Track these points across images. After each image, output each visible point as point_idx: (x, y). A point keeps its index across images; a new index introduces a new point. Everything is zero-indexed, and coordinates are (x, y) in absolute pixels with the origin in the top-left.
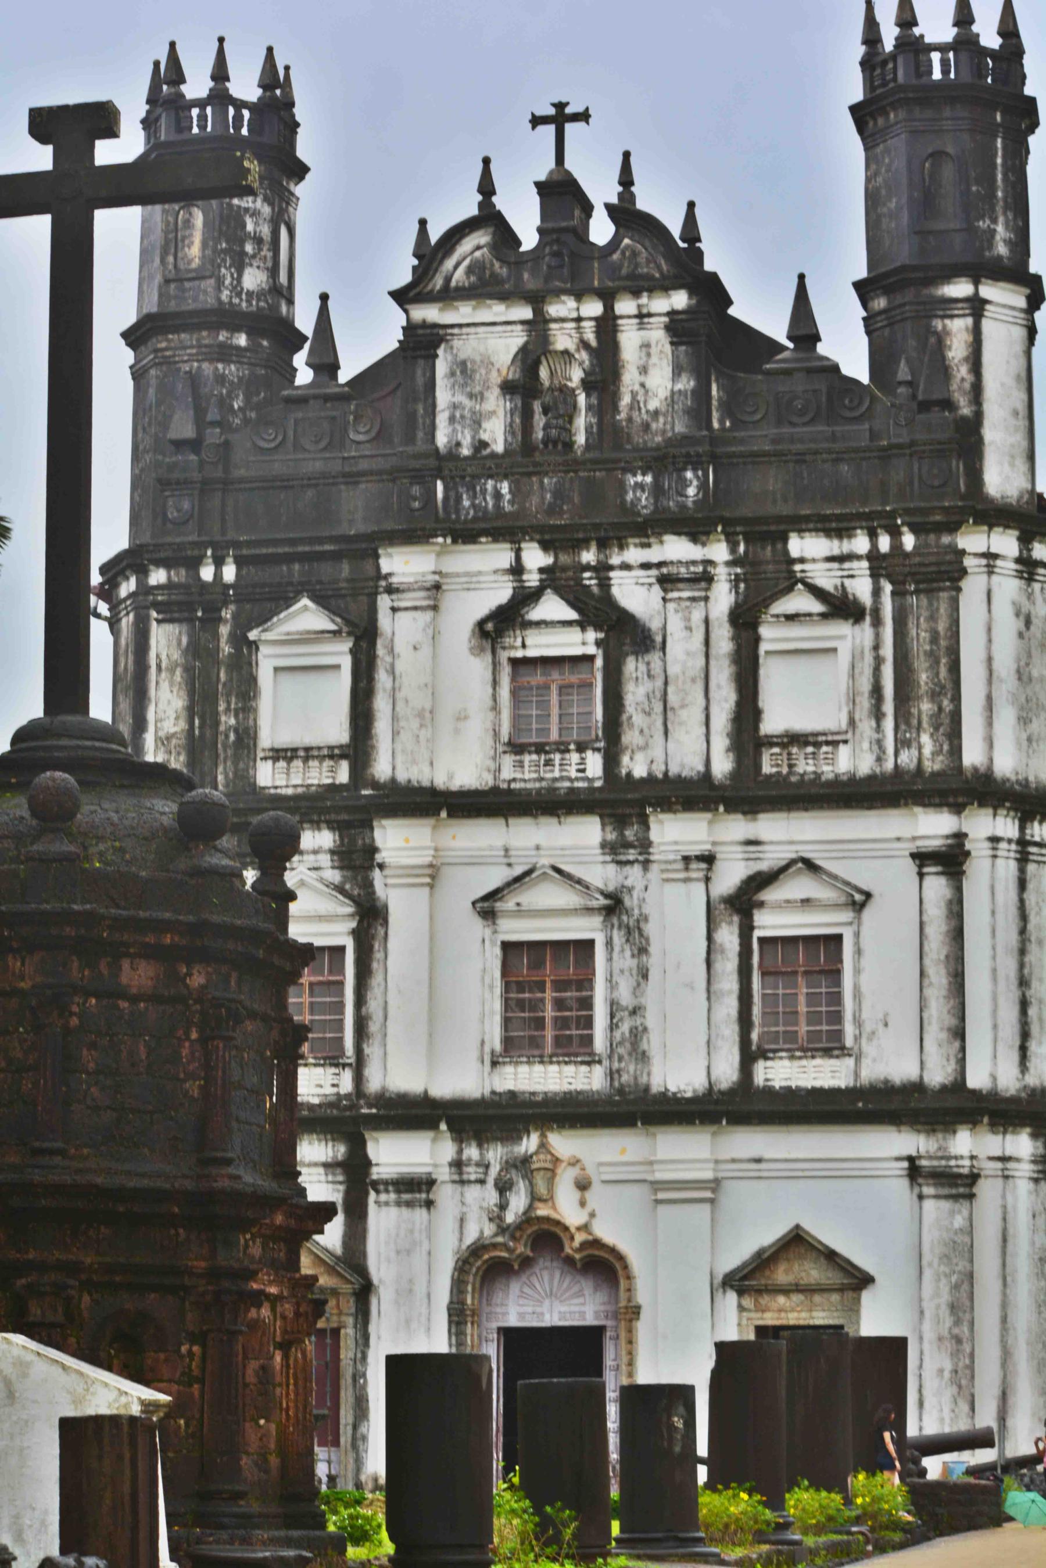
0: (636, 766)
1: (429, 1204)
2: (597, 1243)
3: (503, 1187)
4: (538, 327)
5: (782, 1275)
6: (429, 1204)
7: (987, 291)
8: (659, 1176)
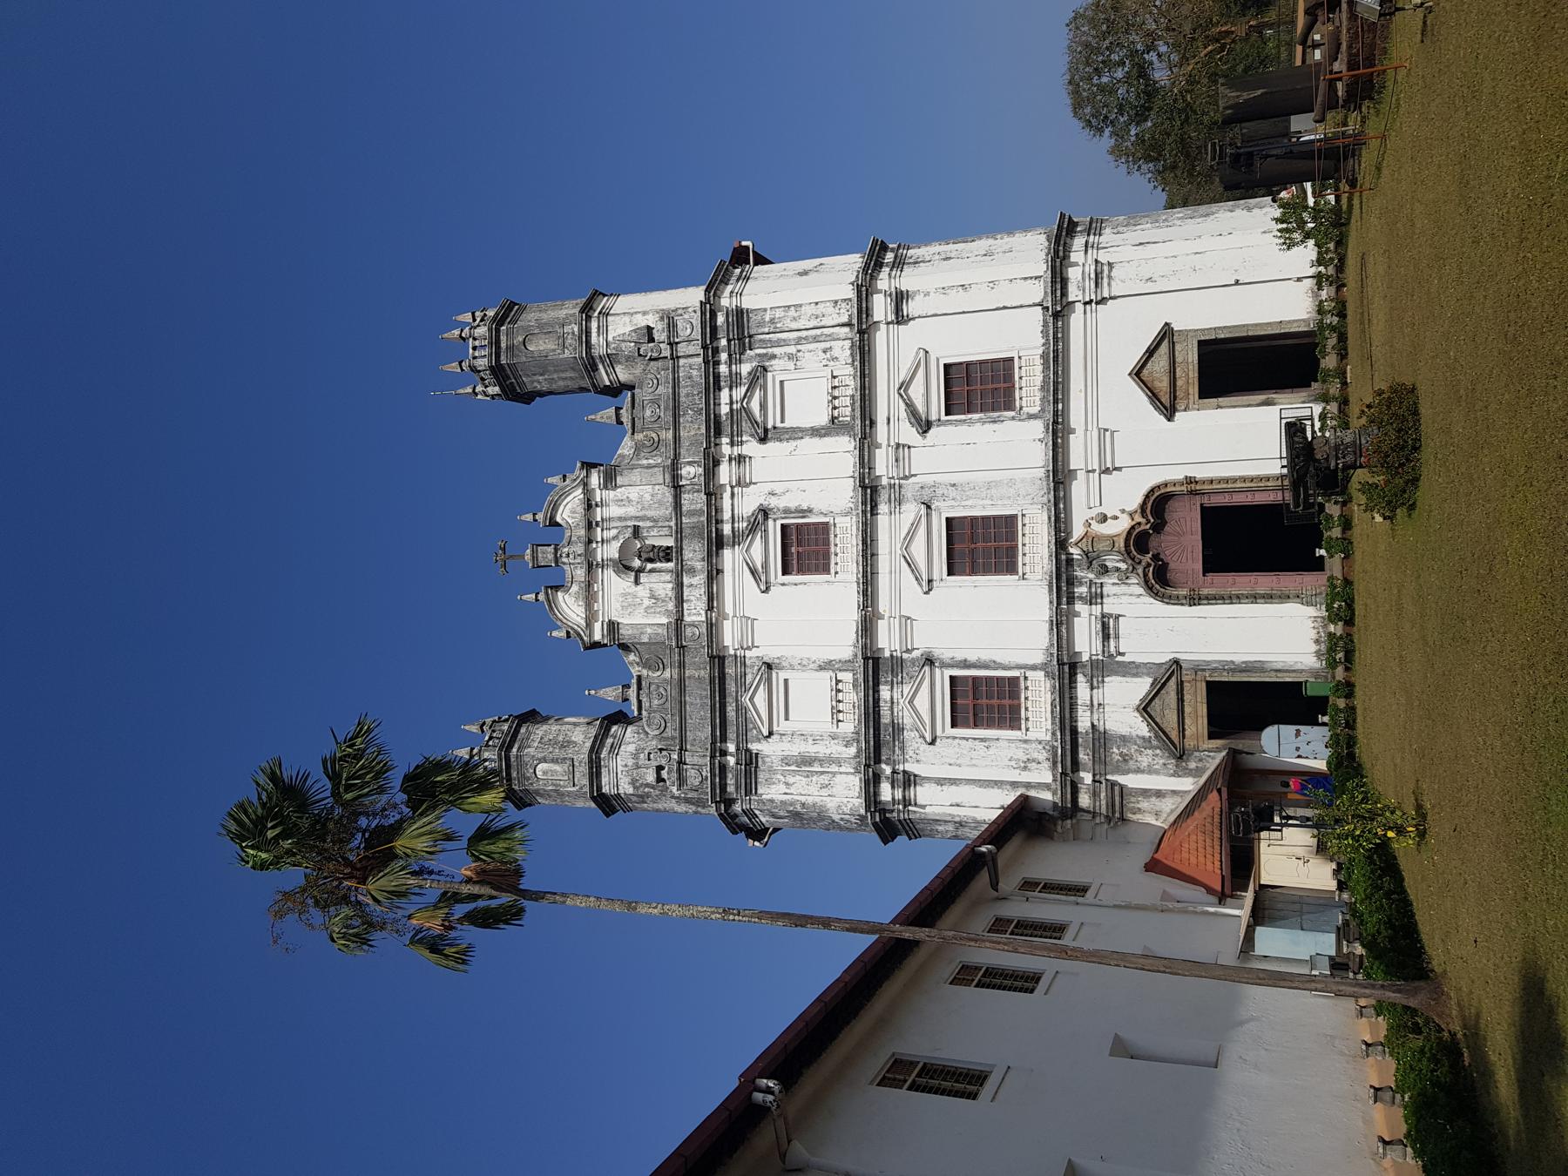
1: (1117, 617)
3: (1105, 570)
6: (1117, 617)
8: (1096, 467)
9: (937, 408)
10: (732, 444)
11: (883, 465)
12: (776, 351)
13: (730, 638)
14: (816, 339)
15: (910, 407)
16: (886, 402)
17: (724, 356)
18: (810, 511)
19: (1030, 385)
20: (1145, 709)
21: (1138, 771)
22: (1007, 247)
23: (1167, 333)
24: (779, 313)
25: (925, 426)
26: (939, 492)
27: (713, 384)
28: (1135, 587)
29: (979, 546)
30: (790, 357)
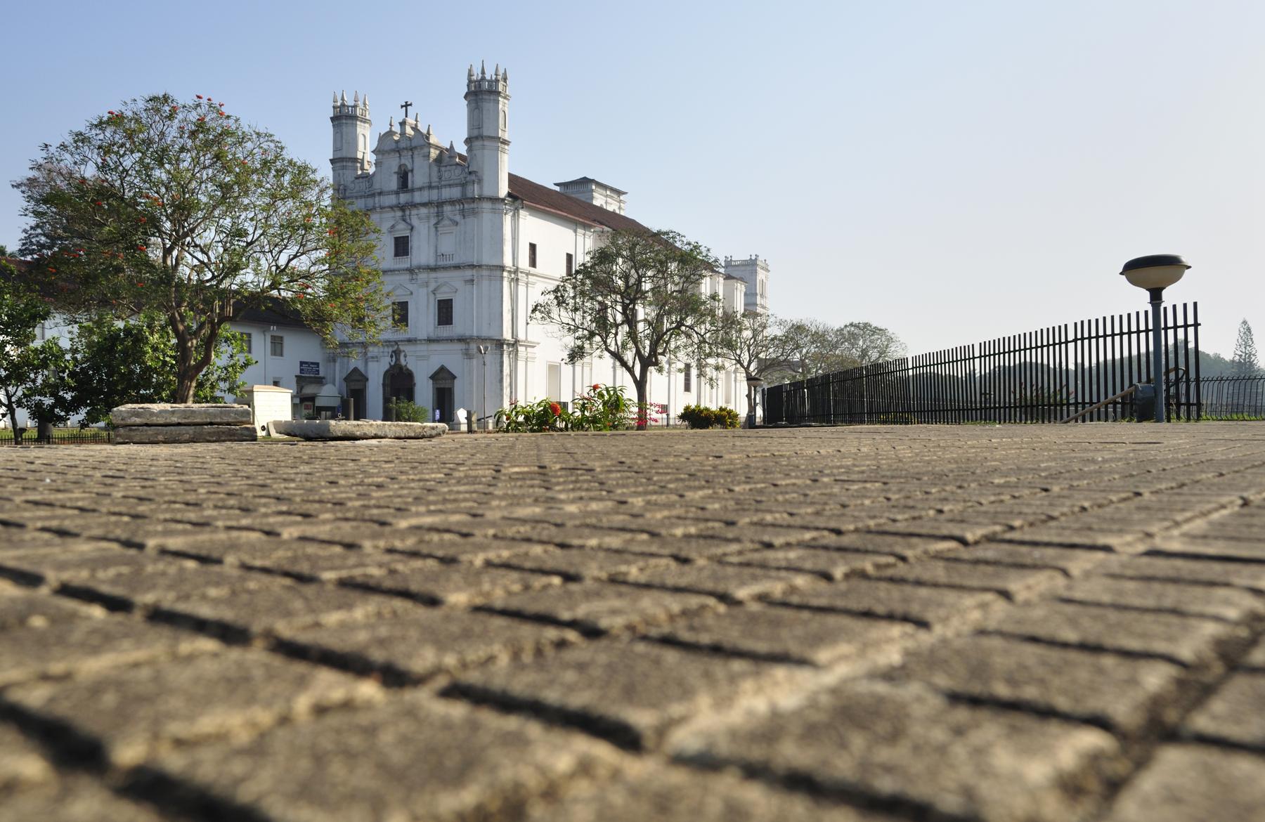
0: (415, 263)
7: (486, 143)
11: (423, 276)
19: (445, 331)
20: (356, 370)
27: (452, 202)
28: (387, 367)
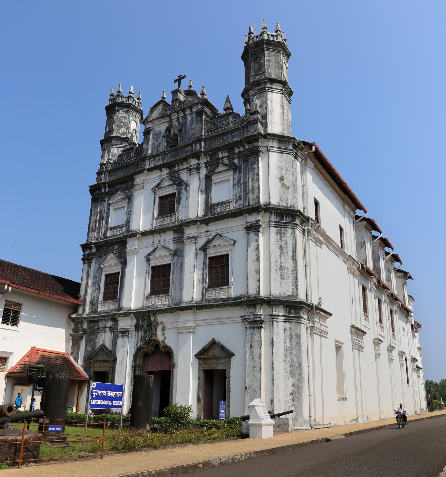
2: (166, 346)
3: (146, 331)
4: (171, 121)
5: (210, 354)
8: (179, 326)
9: (212, 253)
10: (205, 163)
12: (242, 175)
13: (139, 179)
14: (245, 191)
15: (212, 239)
16: (214, 228)
17: (241, 149)
18: (179, 203)
21: (86, 346)
22: (285, 277)
23: (229, 355)
24: (256, 171)
25: (204, 248)
26: (180, 259)
27: (230, 148)
29: (161, 278)
30: (239, 181)
